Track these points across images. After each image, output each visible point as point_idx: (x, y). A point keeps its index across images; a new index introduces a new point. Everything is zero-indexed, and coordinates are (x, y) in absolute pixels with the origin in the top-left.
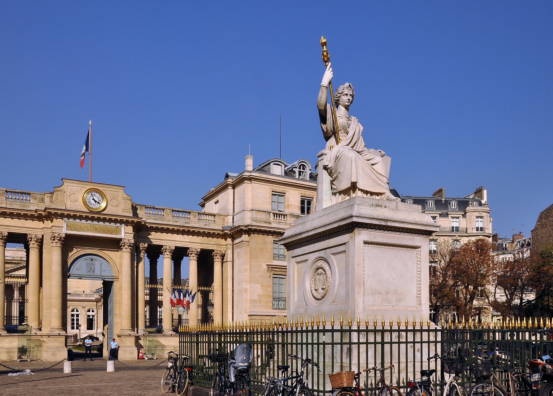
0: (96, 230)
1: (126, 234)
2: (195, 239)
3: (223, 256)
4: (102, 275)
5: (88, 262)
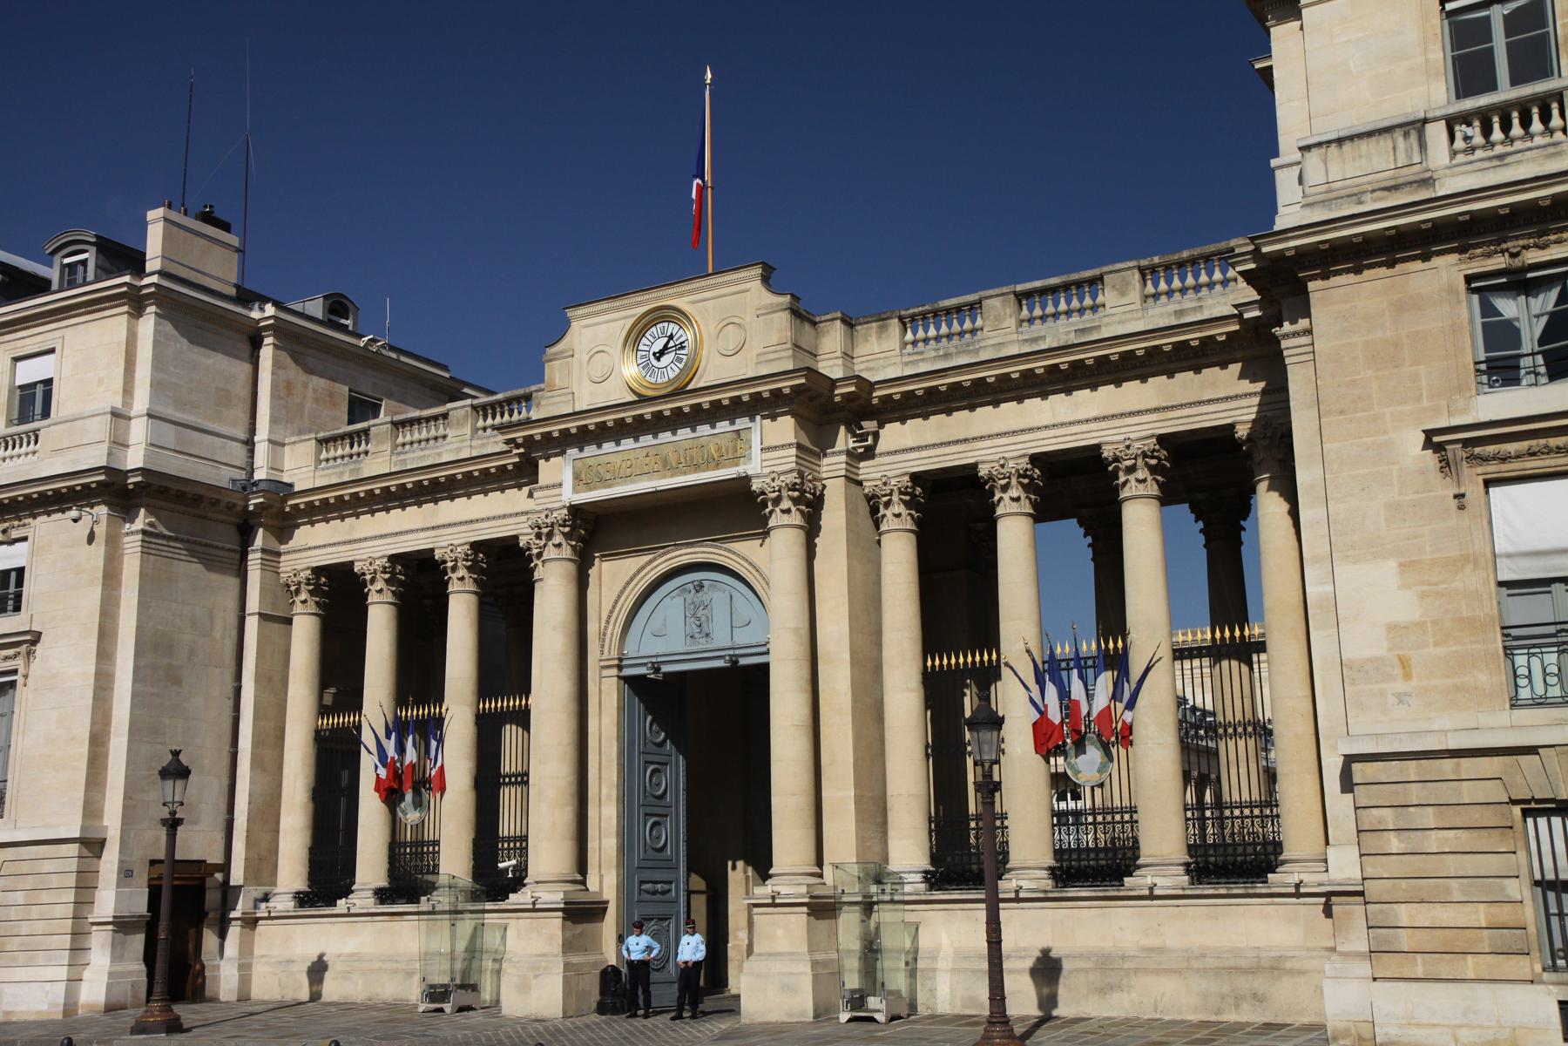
0: (668, 468)
1: (766, 451)
5: (690, 597)
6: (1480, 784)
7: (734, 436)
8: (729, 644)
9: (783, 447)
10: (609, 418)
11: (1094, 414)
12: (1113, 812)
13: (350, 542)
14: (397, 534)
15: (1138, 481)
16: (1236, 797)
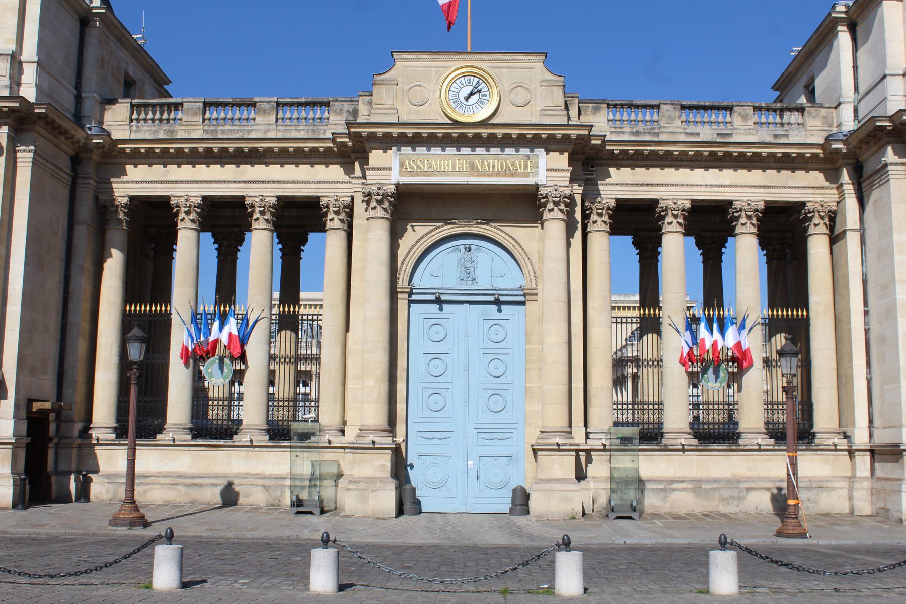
1: (549, 171)
2: (756, 176)
3: (832, 218)
4: (496, 286)
7: (525, 157)
8: (490, 287)
9: (562, 170)
10: (425, 131)
11: (727, 183)
12: (643, 404)
13: (166, 182)
14: (210, 182)
15: (742, 224)
16: (651, 399)
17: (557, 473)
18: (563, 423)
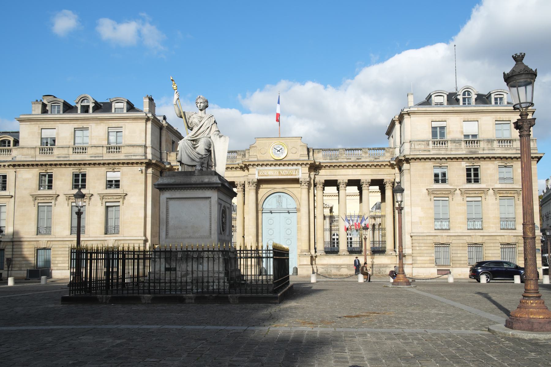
1: (302, 173)
6: (430, 240)
17: (305, 263)
18: (307, 248)
